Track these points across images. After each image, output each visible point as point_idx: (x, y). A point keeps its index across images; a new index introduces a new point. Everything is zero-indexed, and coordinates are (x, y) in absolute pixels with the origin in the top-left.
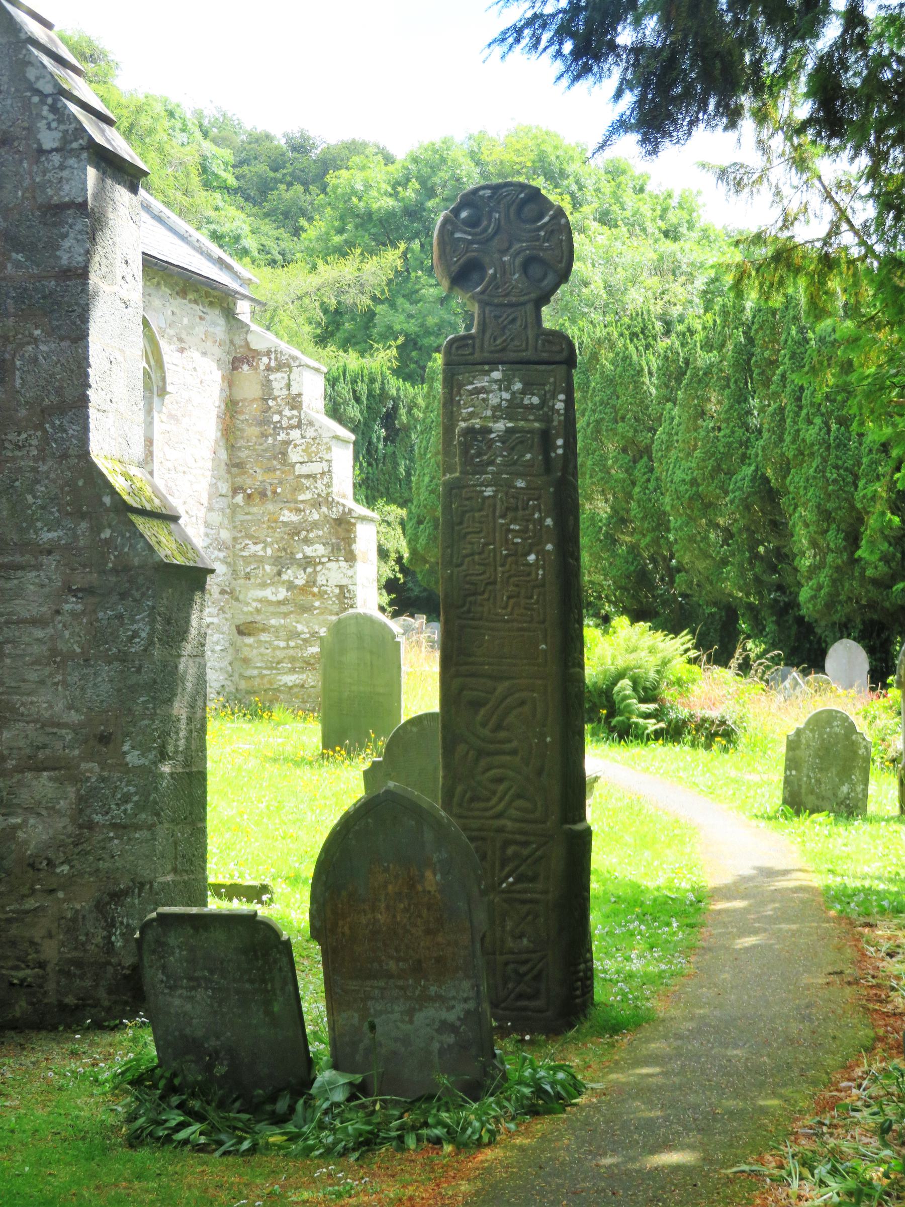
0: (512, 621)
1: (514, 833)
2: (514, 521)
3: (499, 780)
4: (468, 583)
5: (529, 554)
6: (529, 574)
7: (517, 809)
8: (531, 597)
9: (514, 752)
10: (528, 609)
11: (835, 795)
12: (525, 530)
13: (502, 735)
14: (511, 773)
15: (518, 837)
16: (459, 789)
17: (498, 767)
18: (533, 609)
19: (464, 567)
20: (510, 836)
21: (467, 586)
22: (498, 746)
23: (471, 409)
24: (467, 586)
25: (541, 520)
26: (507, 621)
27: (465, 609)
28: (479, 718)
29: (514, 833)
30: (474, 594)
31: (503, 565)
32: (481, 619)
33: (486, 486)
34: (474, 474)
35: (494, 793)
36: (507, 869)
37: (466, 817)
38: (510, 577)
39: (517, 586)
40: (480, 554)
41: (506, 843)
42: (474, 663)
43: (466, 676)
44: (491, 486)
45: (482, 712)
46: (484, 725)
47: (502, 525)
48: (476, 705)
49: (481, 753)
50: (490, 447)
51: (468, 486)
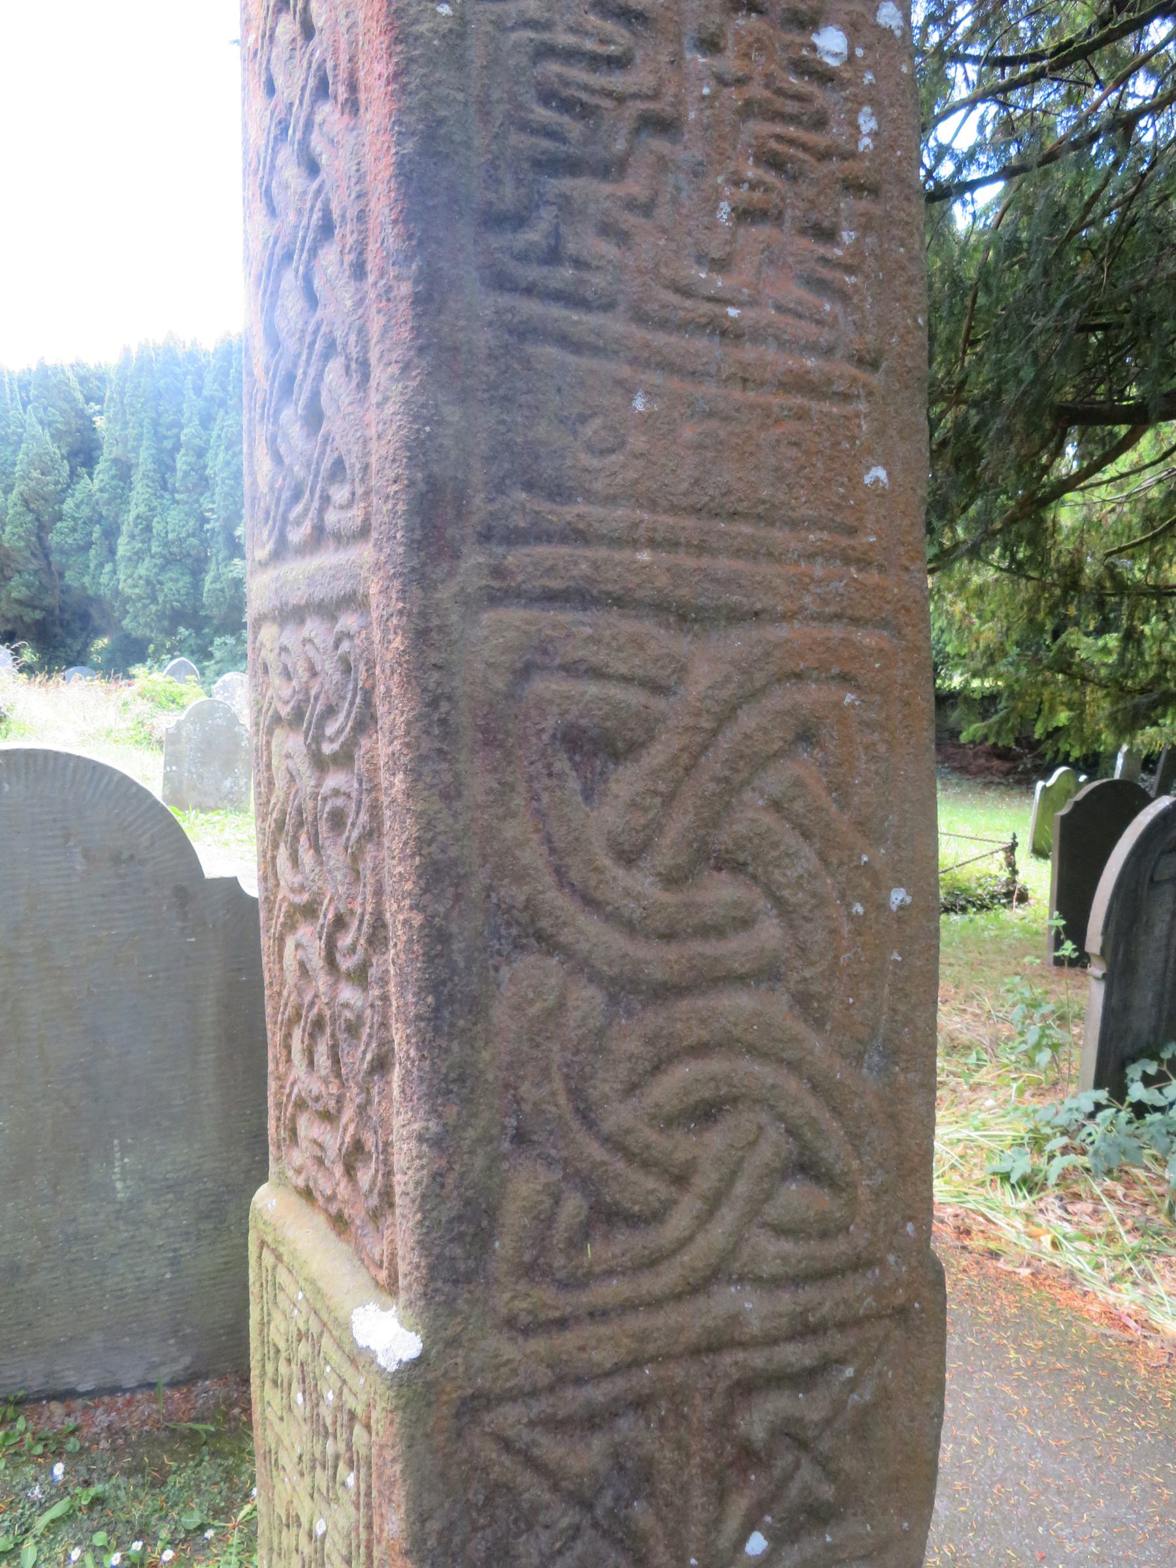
0: (757, 335)
1: (770, 1341)
3: (706, 1113)
4: (547, 97)
6: (820, 122)
7: (780, 1231)
8: (828, 235)
9: (767, 973)
13: (721, 892)
14: (764, 1073)
15: (795, 1355)
16: (526, 1185)
17: (700, 1050)
20: (758, 1359)
21: (543, 114)
22: (697, 947)
27: (534, 236)
29: (770, 1341)
30: (573, 167)
31: (711, 45)
32: (608, 306)
35: (681, 1179)
36: (739, 1505)
37: (562, 1323)
38: (748, 110)
39: (775, 163)
41: (748, 1387)
42: (578, 535)
43: (550, 597)
45: (625, 782)
46: (628, 857)
48: (595, 747)
49: (625, 989)
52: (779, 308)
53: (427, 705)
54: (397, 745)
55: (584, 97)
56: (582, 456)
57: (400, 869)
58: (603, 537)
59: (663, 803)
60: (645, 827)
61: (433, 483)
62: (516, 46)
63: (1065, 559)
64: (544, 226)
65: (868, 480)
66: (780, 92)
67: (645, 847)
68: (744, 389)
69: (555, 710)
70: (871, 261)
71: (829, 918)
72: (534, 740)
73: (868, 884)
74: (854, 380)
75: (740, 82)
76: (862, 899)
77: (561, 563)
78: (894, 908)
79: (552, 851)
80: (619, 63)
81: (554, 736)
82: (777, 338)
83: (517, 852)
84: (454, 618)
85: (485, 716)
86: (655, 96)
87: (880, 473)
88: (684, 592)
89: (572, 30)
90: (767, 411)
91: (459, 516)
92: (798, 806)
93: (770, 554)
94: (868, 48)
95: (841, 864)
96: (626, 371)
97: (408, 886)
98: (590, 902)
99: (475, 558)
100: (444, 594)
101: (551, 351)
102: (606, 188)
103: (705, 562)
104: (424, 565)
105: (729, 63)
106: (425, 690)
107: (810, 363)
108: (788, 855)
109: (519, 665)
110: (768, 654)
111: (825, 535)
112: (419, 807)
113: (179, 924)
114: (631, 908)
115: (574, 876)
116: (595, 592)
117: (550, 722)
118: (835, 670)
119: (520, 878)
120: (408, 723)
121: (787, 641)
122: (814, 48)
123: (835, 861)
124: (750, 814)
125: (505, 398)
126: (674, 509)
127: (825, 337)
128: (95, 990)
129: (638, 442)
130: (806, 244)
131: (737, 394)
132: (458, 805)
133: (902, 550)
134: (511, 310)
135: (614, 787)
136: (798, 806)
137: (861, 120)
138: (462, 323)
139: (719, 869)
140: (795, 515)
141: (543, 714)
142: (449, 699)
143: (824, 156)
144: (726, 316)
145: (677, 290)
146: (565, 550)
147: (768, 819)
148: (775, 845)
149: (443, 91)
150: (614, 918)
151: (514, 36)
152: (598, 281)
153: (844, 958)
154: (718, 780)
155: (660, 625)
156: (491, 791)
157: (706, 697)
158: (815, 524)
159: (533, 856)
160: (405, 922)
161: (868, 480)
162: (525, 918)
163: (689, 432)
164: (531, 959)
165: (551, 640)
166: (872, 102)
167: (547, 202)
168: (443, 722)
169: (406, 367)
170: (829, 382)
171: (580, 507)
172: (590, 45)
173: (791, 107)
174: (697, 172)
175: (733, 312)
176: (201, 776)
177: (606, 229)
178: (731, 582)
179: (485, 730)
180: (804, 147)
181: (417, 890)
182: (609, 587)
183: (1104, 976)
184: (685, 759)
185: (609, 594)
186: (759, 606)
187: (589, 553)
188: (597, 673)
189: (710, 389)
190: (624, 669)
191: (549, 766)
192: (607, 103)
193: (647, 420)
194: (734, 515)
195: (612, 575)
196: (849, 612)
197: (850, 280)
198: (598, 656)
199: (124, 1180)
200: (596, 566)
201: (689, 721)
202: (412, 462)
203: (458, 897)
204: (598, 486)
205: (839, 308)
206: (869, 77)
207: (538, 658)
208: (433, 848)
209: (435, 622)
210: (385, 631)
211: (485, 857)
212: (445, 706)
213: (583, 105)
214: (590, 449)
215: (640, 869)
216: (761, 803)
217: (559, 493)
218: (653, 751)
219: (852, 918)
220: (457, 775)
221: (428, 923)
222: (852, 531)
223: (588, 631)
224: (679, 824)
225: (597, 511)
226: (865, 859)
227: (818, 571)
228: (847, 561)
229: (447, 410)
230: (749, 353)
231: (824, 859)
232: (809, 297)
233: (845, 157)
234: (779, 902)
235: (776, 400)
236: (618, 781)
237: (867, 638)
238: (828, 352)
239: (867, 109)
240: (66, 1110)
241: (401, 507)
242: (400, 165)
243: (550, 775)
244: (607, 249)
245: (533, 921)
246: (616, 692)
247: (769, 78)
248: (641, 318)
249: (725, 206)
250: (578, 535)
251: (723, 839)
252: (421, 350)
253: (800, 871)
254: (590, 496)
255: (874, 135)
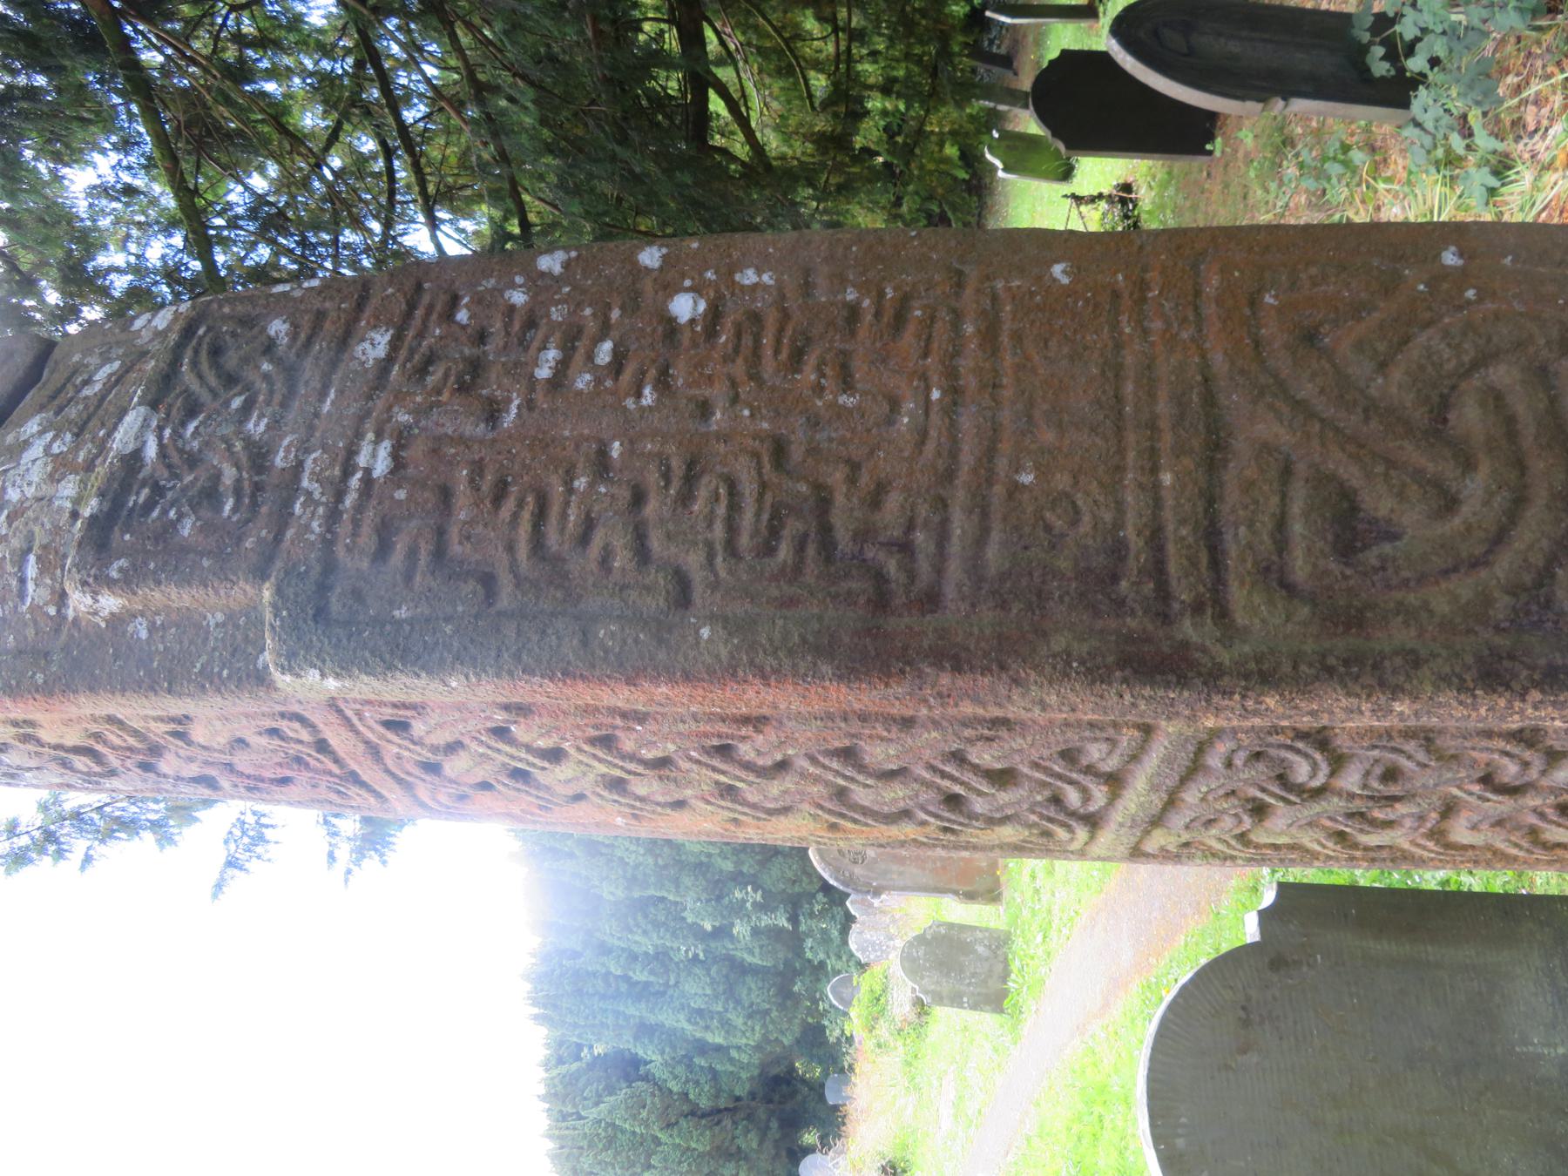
0: (951, 374)
2: (521, 371)
5: (671, 327)
6: (756, 318)
8: (854, 312)
10: (900, 320)
11: (987, 959)
12: (571, 338)
13: (1469, 417)
18: (904, 303)
19: (693, 561)
21: (784, 552)
23: (32, 570)
24: (784, 552)
25: (540, 284)
26: (954, 392)
27: (892, 567)
28: (1413, 518)
30: (826, 529)
31: (704, 409)
33: (348, 469)
34: (283, 518)
38: (755, 376)
39: (797, 357)
40: (638, 498)
42: (1155, 537)
43: (1216, 563)
44: (352, 452)
45: (1379, 503)
46: (1449, 503)
47: (529, 405)
48: (1349, 530)
50: (193, 461)
51: (328, 543)
52: (925, 355)
53: (1331, 676)
54: (1366, 707)
55: (765, 517)
56: (1082, 530)
57: (1483, 711)
58: (1153, 513)
59: (1396, 469)
60: (1421, 486)
61: (1124, 662)
62: (730, 572)
63: (810, 147)
64: (881, 556)
65: (1065, 280)
66: (736, 350)
67: (1437, 484)
68: (1001, 386)
69: (1321, 562)
70: (870, 274)
71: (1484, 320)
72: (1352, 582)
73: (1445, 286)
74: (978, 291)
75: (734, 384)
76: (1461, 291)
77: (1184, 552)
78: (1460, 262)
79: (1455, 569)
80: (732, 485)
81: (1346, 564)
82: (952, 357)
83: (1463, 601)
84: (1247, 649)
85: (1336, 625)
86: (756, 455)
87: (1057, 270)
88: (1196, 443)
89: (710, 525)
90: (1019, 367)
91: (1148, 640)
92: (1382, 347)
93: (1149, 367)
94: (683, 276)
95: (1429, 308)
96: (999, 490)
97: (1502, 703)
98: (1499, 538)
99: (1187, 629)
100: (1225, 657)
101: (992, 553)
102: (839, 499)
103: (1164, 424)
104: (1200, 674)
105: (717, 393)
106: (1317, 678)
107: (969, 329)
108: (1429, 357)
109: (1284, 593)
110: (1242, 372)
111: (1124, 318)
112: (1429, 689)
113: (1305, 969)
114: (1501, 500)
115: (1478, 551)
116: (1206, 523)
117: (1333, 566)
118: (1247, 312)
119: (1487, 601)
120: (1348, 694)
121: (1226, 353)
122: (692, 321)
123: (1428, 315)
124: (1394, 390)
125: (1039, 595)
126: (1121, 451)
127: (944, 315)
128: (1371, 1056)
129: (1062, 481)
130: (863, 332)
131: (1007, 393)
132: (1423, 653)
133: (1123, 251)
134: (959, 586)
135: (1383, 512)
136: (1382, 347)
137: (747, 282)
138: (976, 631)
139: (1445, 421)
140: (1111, 344)
141: (1326, 573)
142: (1324, 656)
143: (786, 315)
144: (940, 400)
145: (923, 443)
146: (1171, 548)
147: (1397, 374)
148: (1422, 368)
149: (777, 636)
150: (1513, 513)
151: (723, 574)
152: (923, 511)
153: (1518, 307)
154: (1367, 419)
155: (1225, 467)
156: (1406, 624)
157: (1290, 426)
158: (1115, 326)
159: (1464, 587)
160: (1536, 708)
161: (1065, 280)
162: (1524, 597)
163: (1049, 436)
164: (1560, 594)
165: (1255, 563)
166: (731, 273)
167: (861, 550)
168: (1346, 663)
169: (1016, 681)
170: (984, 312)
171: (1130, 533)
172: (721, 510)
173: (747, 341)
174: (814, 423)
175: (936, 395)
176: (974, 975)
177: (875, 500)
178: (1180, 401)
179: (1348, 626)
180: (781, 331)
181: (1507, 694)
182: (1200, 509)
183: (1285, 99)
184: (1351, 448)
185: (1206, 511)
186: (1199, 378)
187: (1171, 527)
188: (1281, 524)
189: (1005, 416)
190: (1275, 500)
191: (1376, 570)
192: (768, 498)
193: (1042, 472)
194: (1119, 399)
195: (1188, 507)
196: (1190, 298)
197: (889, 293)
198: (1265, 522)
199: (1555, 1046)
200: (1183, 522)
201: (1315, 443)
202: (1106, 679)
203: (1511, 657)
204: (1108, 517)
205: (916, 303)
206: (710, 275)
207: (1274, 576)
208: (1468, 677)
209: (1252, 666)
210: (1256, 713)
211: (1469, 631)
212: (1331, 661)
213: (772, 518)
214: (1075, 522)
215: (1459, 491)
216: (1380, 381)
217: (1118, 550)
218: (1346, 477)
219: (1480, 299)
220: (1396, 653)
221: (1537, 685)
222: (1116, 295)
223: (1242, 530)
224: (1413, 454)
225: (1131, 519)
226: (1421, 287)
227: (1157, 325)
228: (1143, 300)
229: (1056, 648)
230: (970, 382)
231: (1428, 324)
232: (911, 328)
233: (783, 297)
234: (1475, 365)
235: (1008, 360)
236: (1376, 509)
237: (1213, 283)
238: (958, 316)
239: (738, 277)
240: (1489, 1094)
241: (1147, 692)
242: (840, 678)
243: (1383, 568)
244: (893, 502)
245: (1526, 590)
246: (1296, 508)
247: (728, 359)
248: (949, 476)
249: (843, 399)
250: (1155, 537)
251: (1420, 416)
252: (1003, 667)
253: (1442, 346)
254: (1118, 524)
255: (759, 272)
